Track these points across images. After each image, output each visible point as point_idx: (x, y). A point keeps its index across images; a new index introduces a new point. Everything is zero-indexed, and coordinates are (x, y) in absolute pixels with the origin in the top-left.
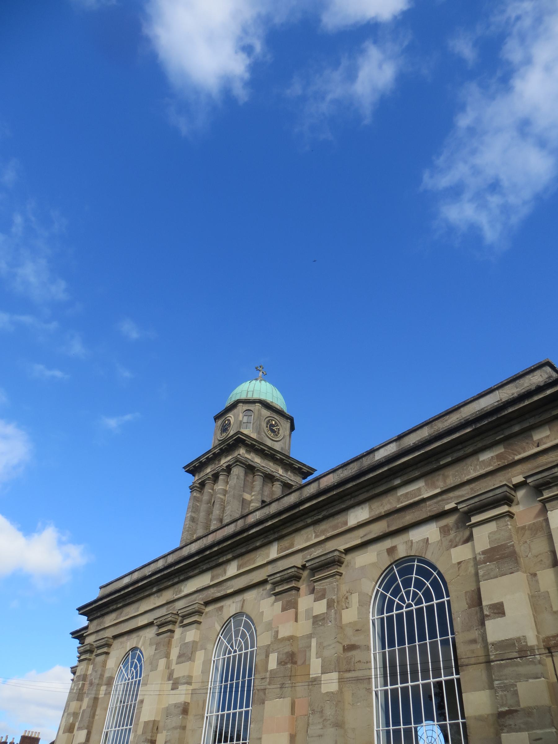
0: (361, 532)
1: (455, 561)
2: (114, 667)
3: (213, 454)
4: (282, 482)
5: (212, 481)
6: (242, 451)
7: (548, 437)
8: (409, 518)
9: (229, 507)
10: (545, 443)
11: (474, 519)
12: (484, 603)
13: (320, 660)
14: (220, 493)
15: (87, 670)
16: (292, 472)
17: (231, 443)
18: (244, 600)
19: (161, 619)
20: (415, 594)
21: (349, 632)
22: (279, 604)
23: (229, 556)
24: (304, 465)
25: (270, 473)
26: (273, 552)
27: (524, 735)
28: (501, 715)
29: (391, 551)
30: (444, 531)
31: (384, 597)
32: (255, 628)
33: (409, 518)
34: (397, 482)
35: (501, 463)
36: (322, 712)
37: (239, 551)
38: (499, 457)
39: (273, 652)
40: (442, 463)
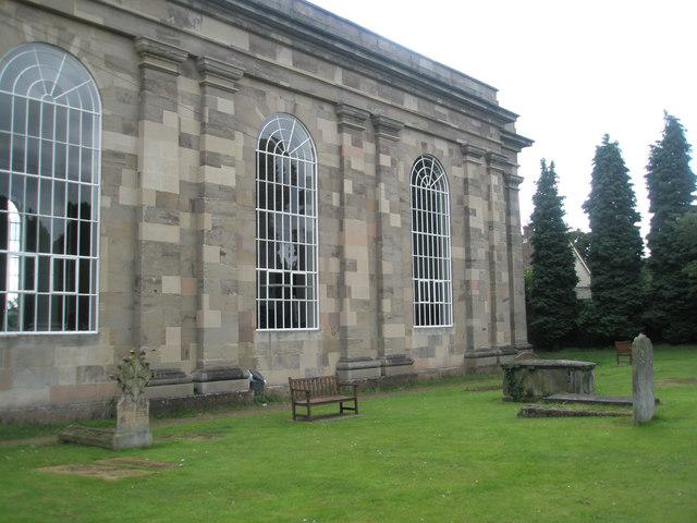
8: (439, 131)
11: (469, 158)
23: (288, 41)
26: (338, 78)
33: (439, 131)
37: (301, 45)
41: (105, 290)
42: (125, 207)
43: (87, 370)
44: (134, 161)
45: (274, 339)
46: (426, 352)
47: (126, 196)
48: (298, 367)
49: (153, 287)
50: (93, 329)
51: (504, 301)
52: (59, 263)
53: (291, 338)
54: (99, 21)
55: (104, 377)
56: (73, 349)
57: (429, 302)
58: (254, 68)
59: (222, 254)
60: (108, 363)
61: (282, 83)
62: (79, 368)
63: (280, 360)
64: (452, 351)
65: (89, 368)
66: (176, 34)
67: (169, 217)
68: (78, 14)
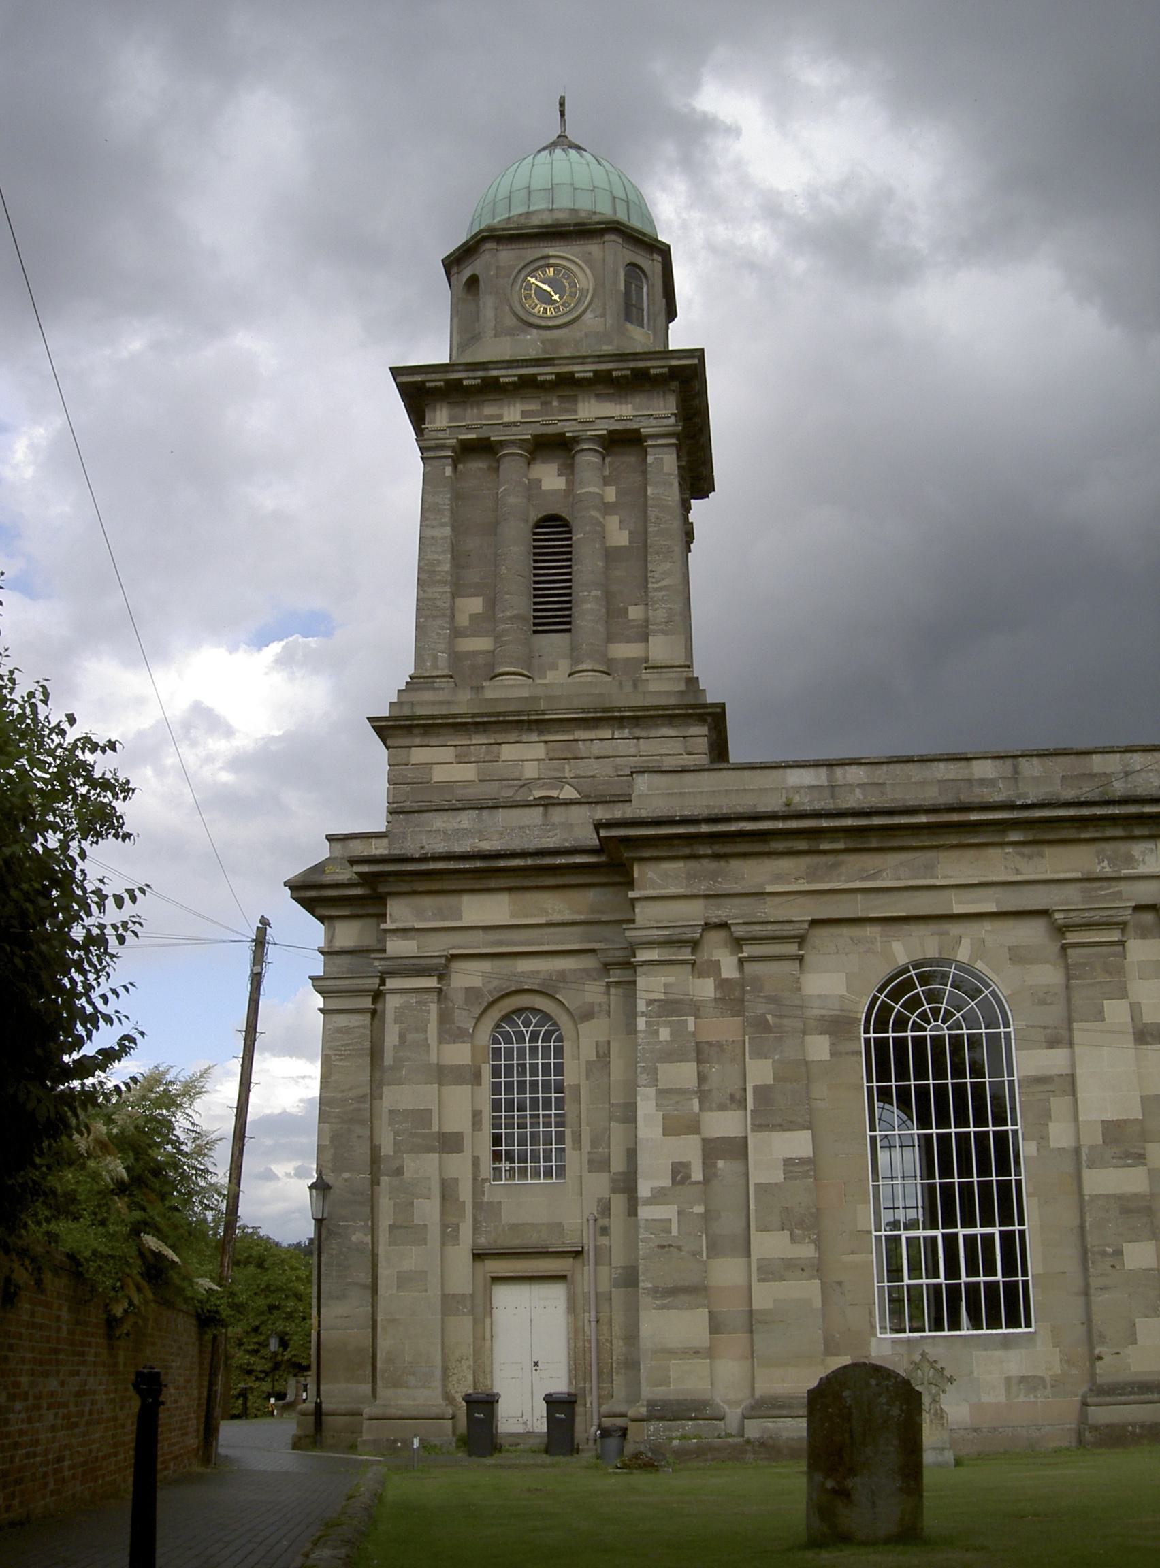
5: (526, 451)
17: (653, 371)
19: (1092, 913)
41: (1040, 1271)
42: (1061, 1151)
43: (1020, 1382)
44: (1070, 1083)
47: (1060, 1134)
50: (1028, 1325)
52: (970, 1240)
54: (992, 908)
55: (1049, 1391)
56: (999, 1353)
60: (1051, 1373)
62: (1008, 1379)
65: (1023, 1379)
66: (1113, 884)
67: (1128, 1155)
68: (958, 909)
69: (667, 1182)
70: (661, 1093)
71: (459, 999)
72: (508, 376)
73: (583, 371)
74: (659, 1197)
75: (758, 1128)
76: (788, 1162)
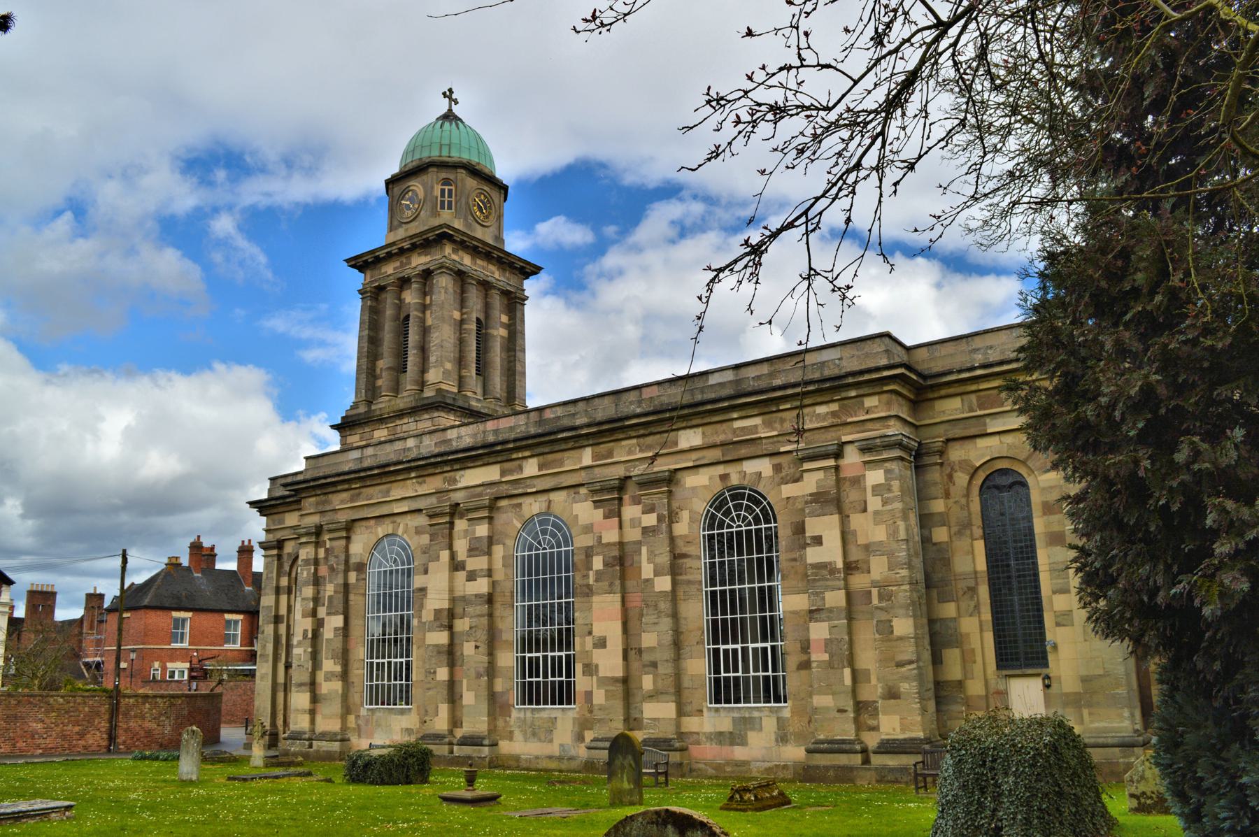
0: (694, 456)
1: (784, 496)
2: (361, 551)
3: (399, 249)
4: (499, 289)
6: (448, 249)
7: (876, 407)
8: (744, 451)
9: (437, 334)
10: (873, 412)
11: (806, 466)
12: (807, 535)
13: (652, 565)
14: (416, 310)
15: (316, 553)
16: (510, 273)
18: (550, 501)
20: (745, 518)
21: (680, 543)
22: (600, 512)
23: (527, 453)
24: (528, 263)
25: (485, 278)
26: (587, 457)
27: (827, 624)
28: (811, 612)
29: (724, 477)
30: (778, 468)
31: (713, 517)
32: (568, 529)
34: (735, 415)
35: (836, 421)
36: (656, 606)
38: (834, 414)
39: (597, 554)
40: (781, 408)
45: (529, 714)
46: (735, 738)
48: (551, 741)
49: (432, 676)
51: (900, 665)
53: (544, 715)
57: (541, 679)
58: (504, 489)
59: (477, 647)
61: (529, 490)
63: (534, 734)
64: (782, 738)
68: (396, 511)
69: (301, 638)
70: (303, 599)
71: (285, 557)
72: (382, 254)
73: (406, 245)
74: (299, 643)
75: (328, 614)
76: (336, 629)
